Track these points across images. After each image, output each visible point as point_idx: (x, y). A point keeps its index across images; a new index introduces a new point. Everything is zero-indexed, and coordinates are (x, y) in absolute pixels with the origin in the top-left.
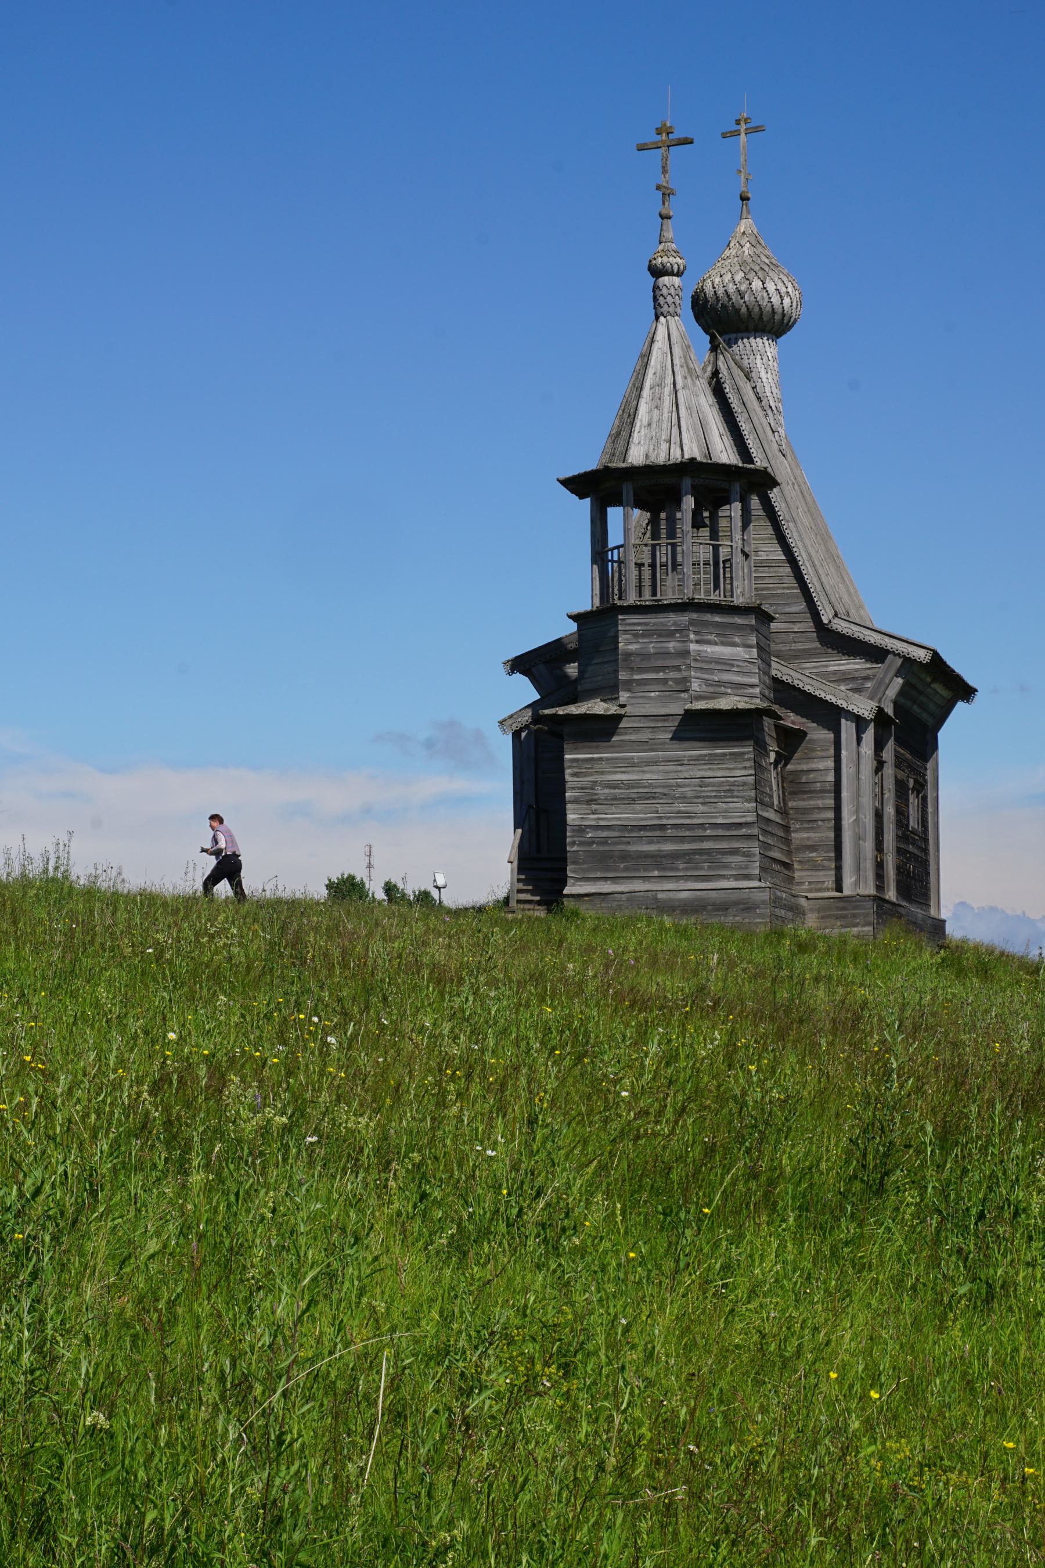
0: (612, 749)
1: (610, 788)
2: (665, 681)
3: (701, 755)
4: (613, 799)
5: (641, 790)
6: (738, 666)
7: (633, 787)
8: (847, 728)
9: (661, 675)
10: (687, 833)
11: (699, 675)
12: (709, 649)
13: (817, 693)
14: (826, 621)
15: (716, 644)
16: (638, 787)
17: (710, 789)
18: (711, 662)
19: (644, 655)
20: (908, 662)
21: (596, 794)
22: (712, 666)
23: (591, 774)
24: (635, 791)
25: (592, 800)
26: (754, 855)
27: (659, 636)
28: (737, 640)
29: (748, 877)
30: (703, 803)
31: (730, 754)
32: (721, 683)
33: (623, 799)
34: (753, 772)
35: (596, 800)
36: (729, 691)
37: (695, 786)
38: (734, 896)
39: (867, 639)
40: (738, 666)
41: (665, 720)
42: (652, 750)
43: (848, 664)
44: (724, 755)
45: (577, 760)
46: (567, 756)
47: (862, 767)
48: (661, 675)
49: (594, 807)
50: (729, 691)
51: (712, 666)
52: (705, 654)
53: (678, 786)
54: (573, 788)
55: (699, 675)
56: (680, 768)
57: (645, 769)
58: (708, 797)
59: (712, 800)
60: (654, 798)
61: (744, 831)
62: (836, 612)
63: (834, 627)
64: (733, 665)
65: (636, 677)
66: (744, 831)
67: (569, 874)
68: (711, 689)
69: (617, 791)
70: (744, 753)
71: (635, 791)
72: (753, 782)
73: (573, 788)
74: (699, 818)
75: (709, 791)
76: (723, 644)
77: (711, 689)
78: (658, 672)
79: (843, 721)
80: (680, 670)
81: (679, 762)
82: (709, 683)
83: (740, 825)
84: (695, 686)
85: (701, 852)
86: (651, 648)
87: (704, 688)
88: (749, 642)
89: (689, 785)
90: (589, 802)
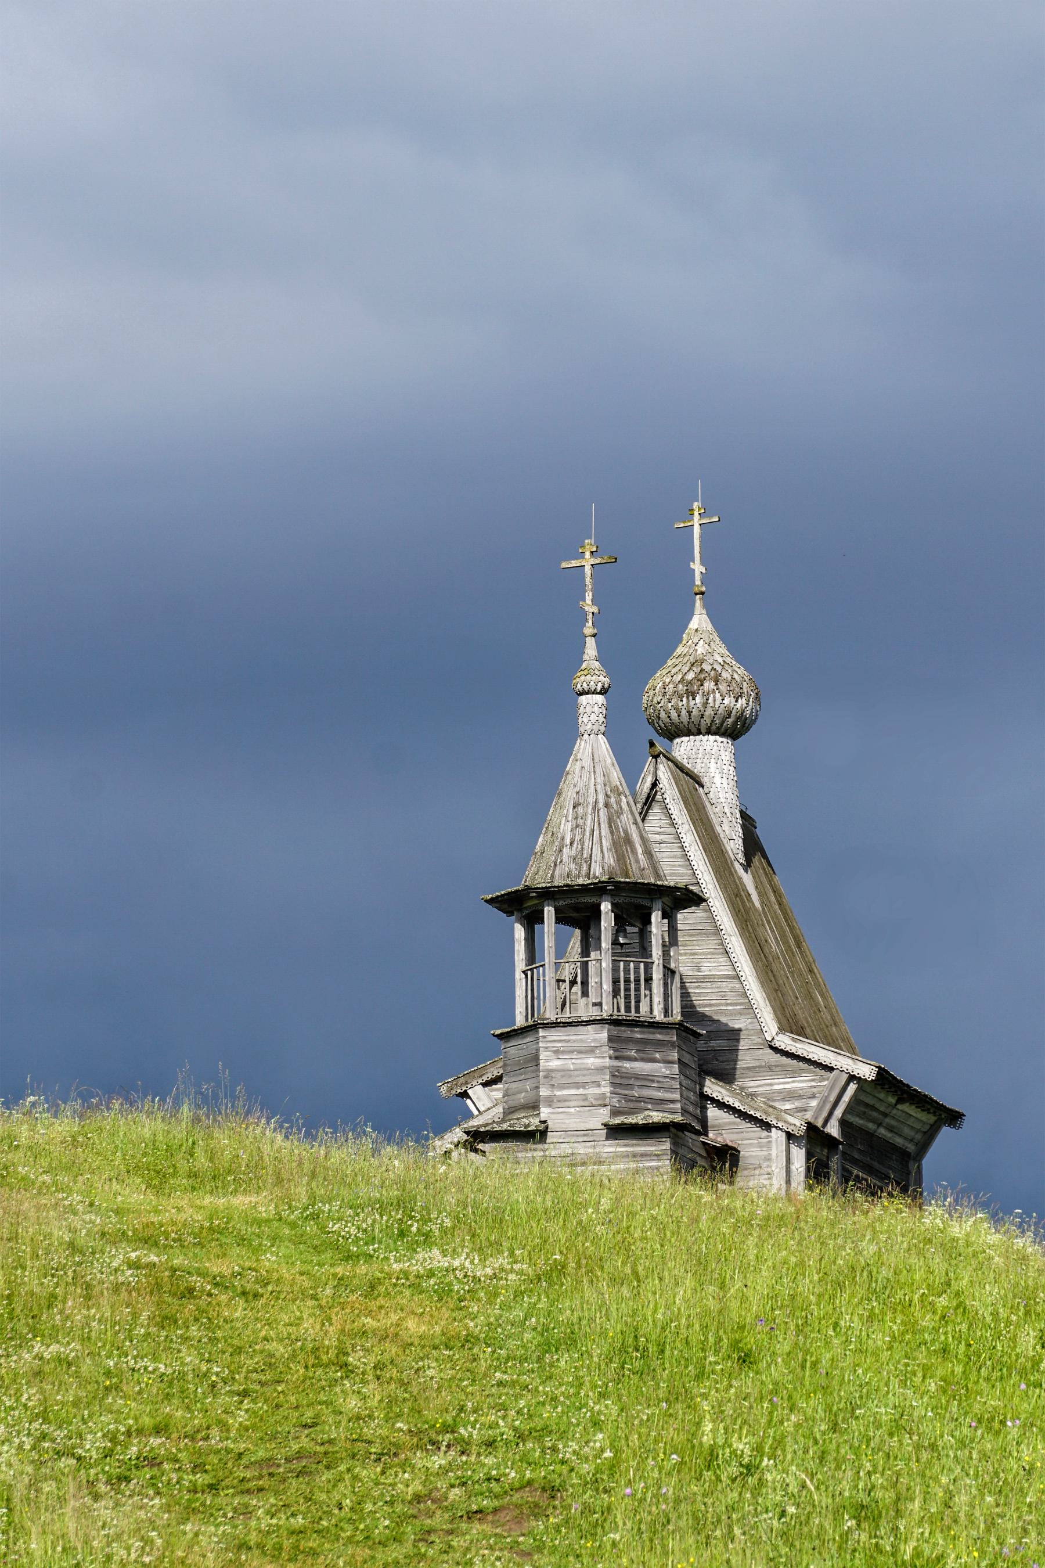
6: (658, 1082)
12: (627, 1065)
15: (636, 1060)
18: (630, 1078)
19: (563, 1071)
27: (580, 1052)
28: (657, 1056)
32: (642, 1099)
36: (649, 1106)
40: (658, 1082)
50: (649, 1106)
51: (632, 1082)
64: (653, 1081)
68: (631, 1105)
76: (643, 1060)
77: (631, 1105)
80: (599, 1086)
82: (628, 1099)
88: (670, 1058)
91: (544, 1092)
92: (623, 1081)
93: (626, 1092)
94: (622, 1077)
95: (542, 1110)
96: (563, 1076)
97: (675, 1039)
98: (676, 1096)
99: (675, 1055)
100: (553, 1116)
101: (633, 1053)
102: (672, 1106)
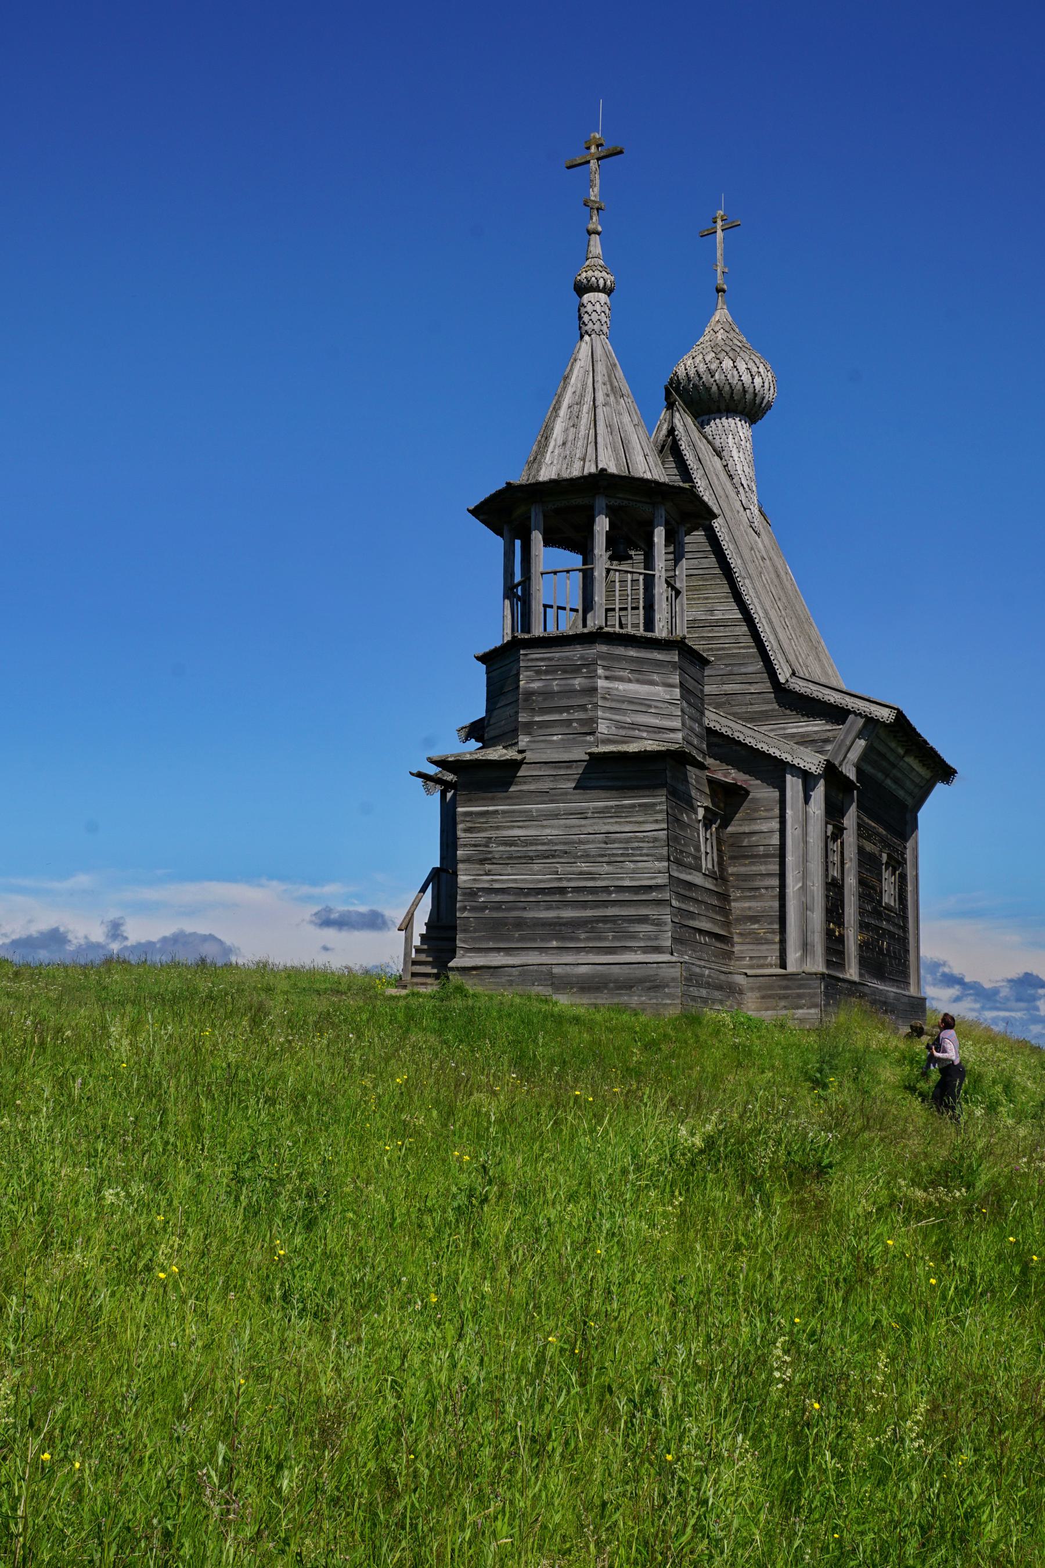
0: (509, 801)
1: (505, 844)
2: (569, 722)
3: (606, 807)
4: (509, 858)
5: (540, 848)
6: (656, 707)
7: (532, 844)
8: (793, 785)
9: (565, 716)
10: (590, 898)
11: (608, 715)
12: (621, 686)
13: (759, 746)
14: (782, 681)
15: (630, 681)
16: (537, 844)
17: (616, 845)
18: (623, 702)
19: (547, 694)
20: (871, 721)
21: (490, 852)
22: (624, 706)
23: (485, 830)
24: (534, 848)
25: (486, 859)
26: (666, 924)
27: (565, 672)
28: (655, 677)
29: (658, 950)
30: (609, 863)
31: (640, 805)
32: (634, 726)
33: (520, 857)
34: (665, 826)
35: (490, 859)
36: (645, 735)
37: (600, 842)
38: (639, 972)
39: (826, 698)
40: (656, 707)
41: (568, 767)
42: (552, 802)
43: (807, 726)
44: (633, 806)
45: (470, 814)
46: (459, 809)
47: (810, 829)
48: (565, 716)
49: (488, 867)
50: (645, 735)
51: (624, 706)
52: (616, 692)
53: (581, 842)
54: (465, 845)
55: (608, 715)
56: (583, 822)
57: (545, 823)
58: (613, 855)
59: (619, 859)
60: (553, 856)
61: (654, 895)
62: (793, 670)
63: (792, 686)
64: (650, 706)
65: (537, 719)
66: (654, 895)
67: (459, 944)
68: (623, 732)
69: (513, 848)
70: (655, 804)
71: (534, 848)
72: (665, 837)
73: (465, 845)
74: (604, 879)
75: (616, 848)
76: (638, 681)
77: (623, 732)
78: (561, 713)
79: (788, 777)
80: (586, 710)
81: (582, 815)
82: (620, 725)
83: (650, 888)
84: (603, 728)
85: (605, 919)
86: (555, 686)
87: (614, 730)
88: (671, 681)
89: (593, 842)
90: (482, 862)
91: (523, 718)
92: (613, 705)
93: (617, 717)
94: (613, 700)
95: (521, 737)
96: (545, 700)
97: (676, 659)
98: (677, 724)
99: (676, 679)
100: (533, 746)
101: (625, 674)
102: (672, 735)
